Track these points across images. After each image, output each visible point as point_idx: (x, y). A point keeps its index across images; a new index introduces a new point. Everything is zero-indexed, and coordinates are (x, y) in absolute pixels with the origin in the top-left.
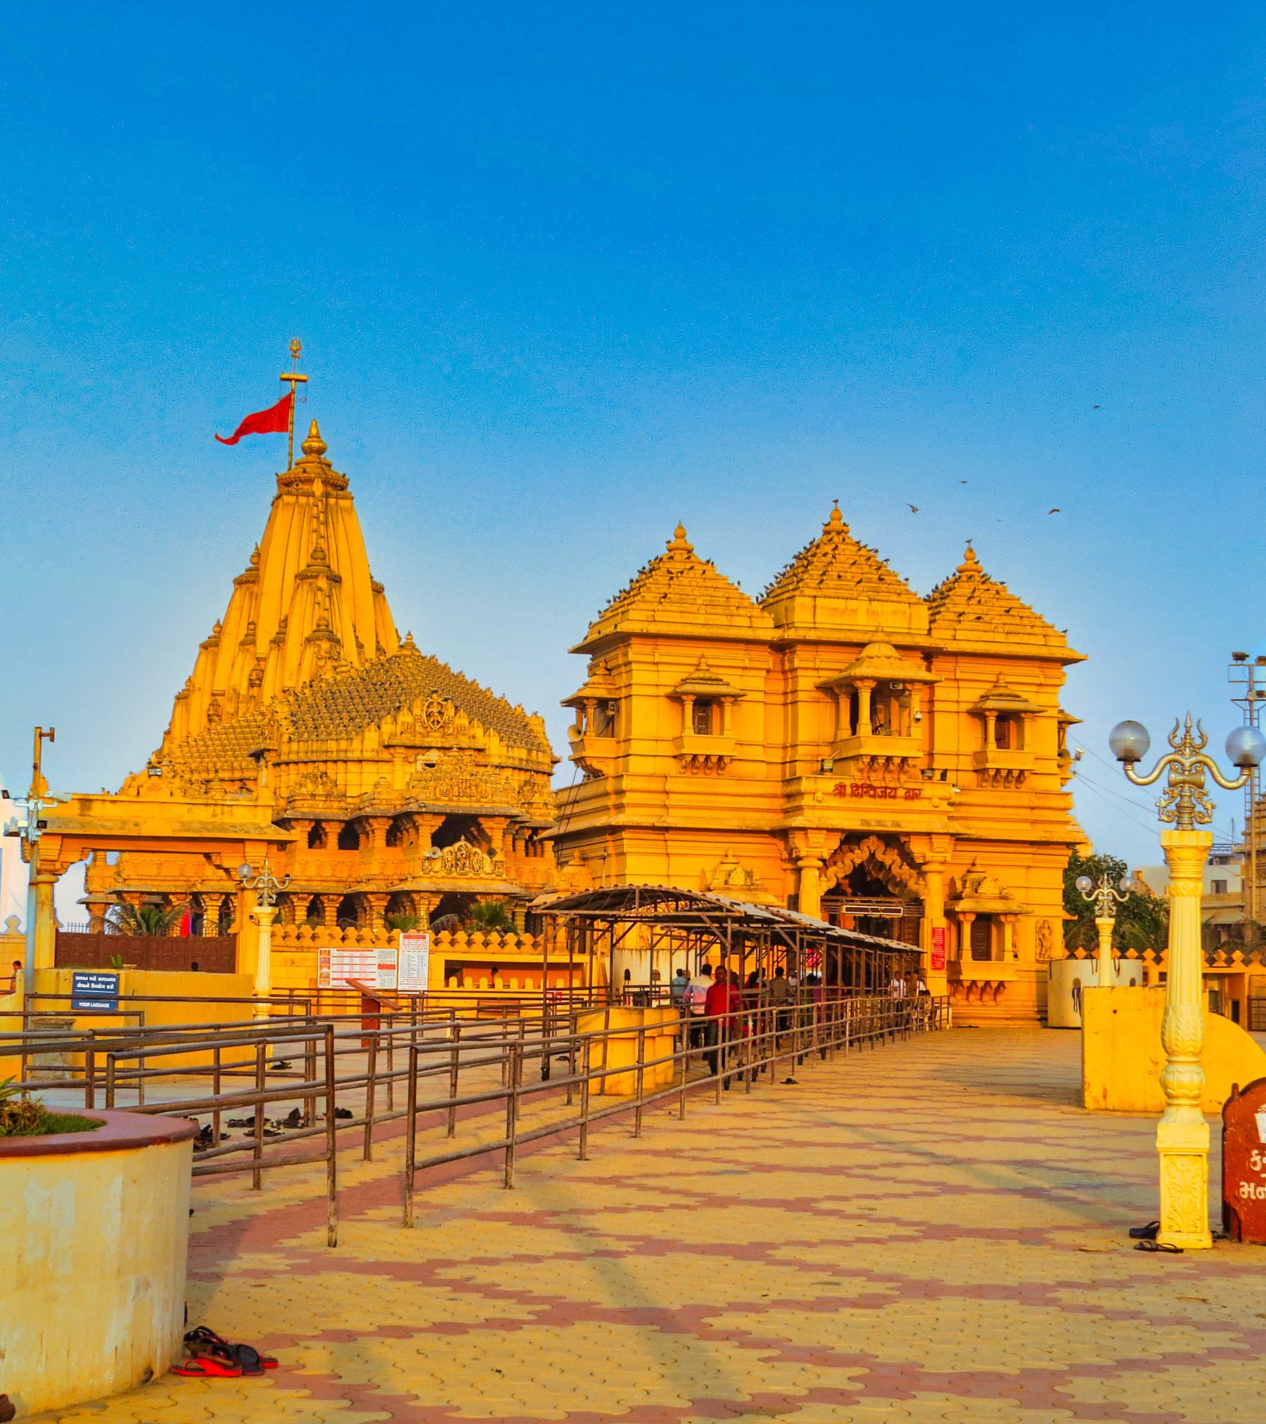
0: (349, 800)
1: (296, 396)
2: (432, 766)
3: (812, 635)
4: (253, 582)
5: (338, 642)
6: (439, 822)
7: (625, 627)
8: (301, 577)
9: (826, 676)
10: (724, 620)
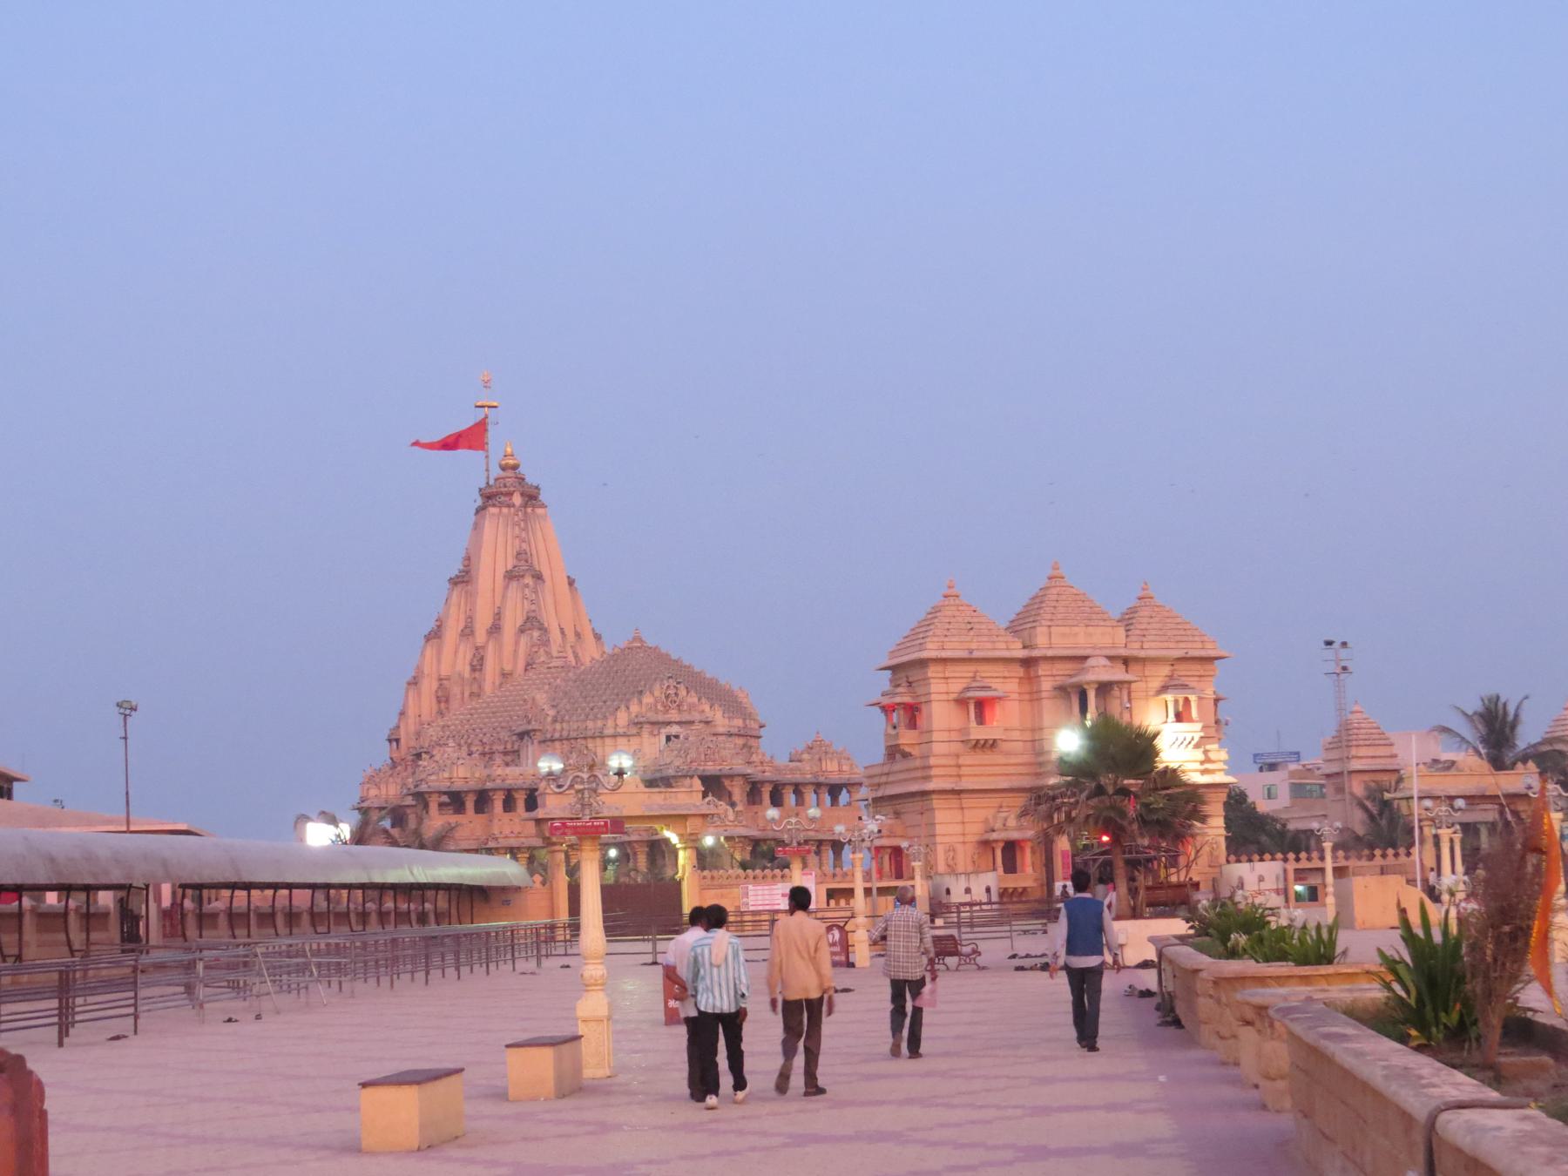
3: (1050, 653)
7: (925, 655)
9: (1060, 681)
10: (989, 646)
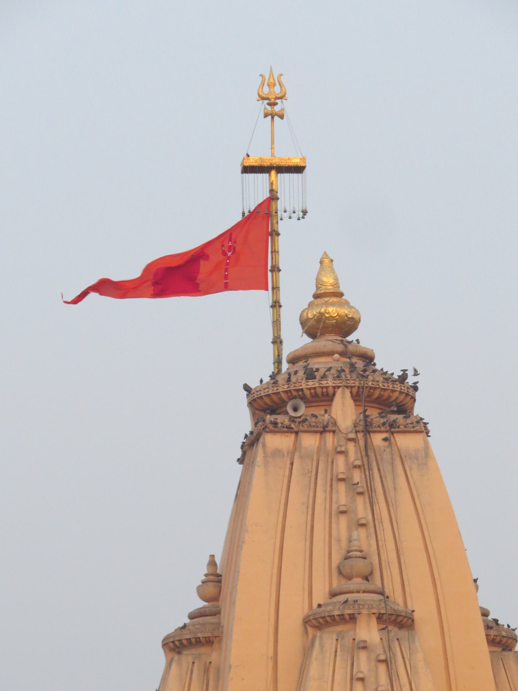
1: (280, 205)
4: (209, 642)
8: (318, 622)
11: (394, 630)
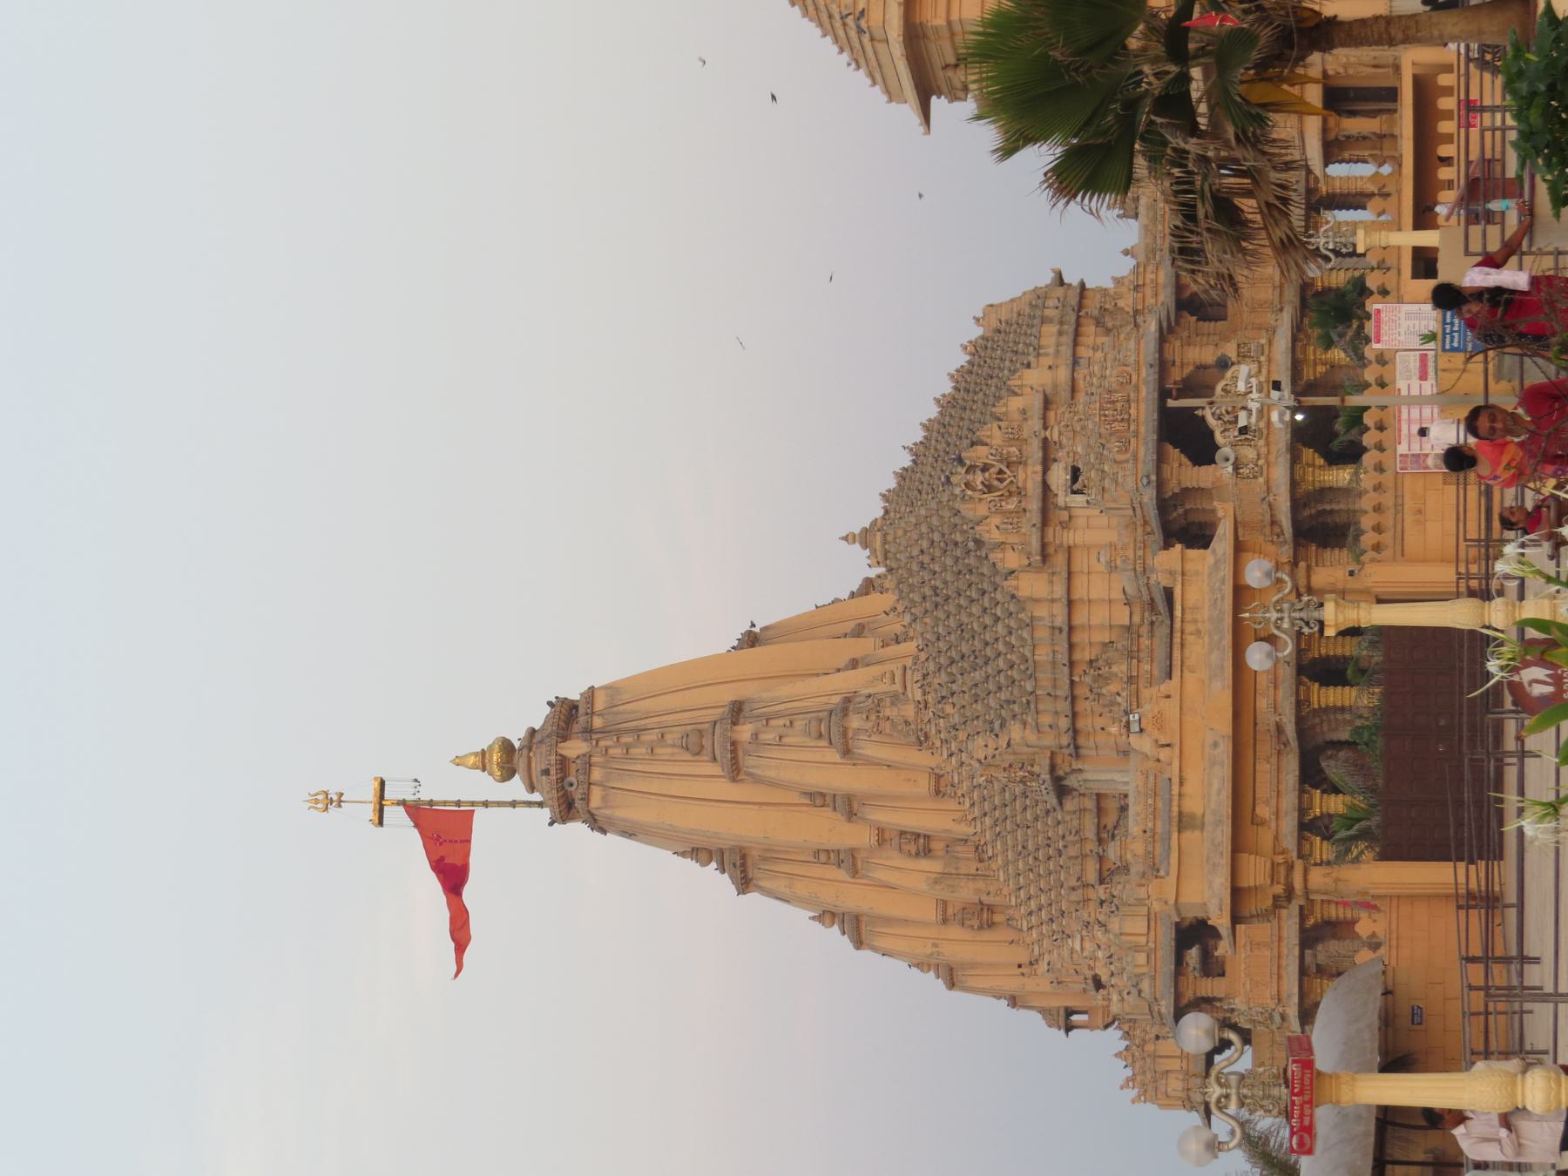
0: (1137, 619)
1: (410, 798)
2: (1075, 473)
4: (743, 857)
5: (848, 700)
6: (1174, 454)
8: (735, 771)
11: (746, 712)
